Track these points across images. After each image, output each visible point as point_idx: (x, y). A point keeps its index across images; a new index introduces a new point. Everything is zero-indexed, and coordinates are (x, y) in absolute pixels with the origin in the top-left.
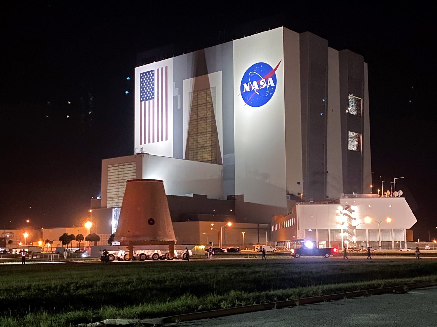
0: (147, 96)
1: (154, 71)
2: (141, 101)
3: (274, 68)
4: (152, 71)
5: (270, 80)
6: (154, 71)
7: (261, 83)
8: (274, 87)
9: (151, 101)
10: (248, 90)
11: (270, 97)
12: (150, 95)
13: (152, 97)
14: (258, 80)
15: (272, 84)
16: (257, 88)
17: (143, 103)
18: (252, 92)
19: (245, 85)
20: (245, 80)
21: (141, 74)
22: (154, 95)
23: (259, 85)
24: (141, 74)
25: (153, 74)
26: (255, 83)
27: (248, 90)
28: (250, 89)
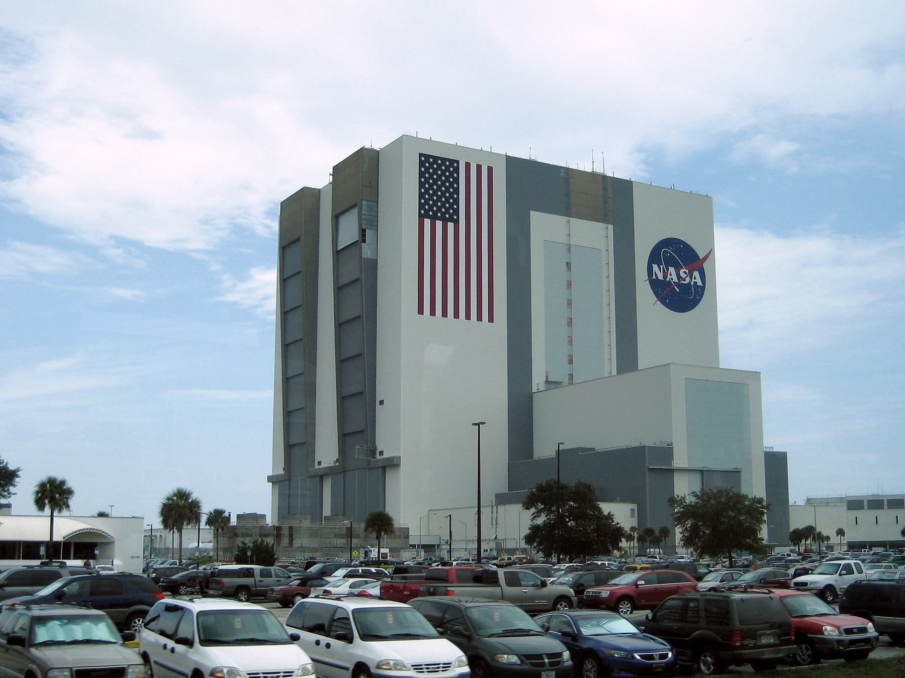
0: (439, 209)
1: (458, 162)
2: (421, 217)
4: (452, 162)
5: (696, 274)
6: (458, 162)
8: (703, 288)
10: (661, 277)
12: (447, 210)
13: (451, 216)
14: (678, 268)
15: (700, 283)
19: (655, 267)
21: (421, 155)
22: (457, 212)
24: (421, 155)
25: (457, 170)
26: (672, 270)
27: (661, 277)
28: (665, 277)
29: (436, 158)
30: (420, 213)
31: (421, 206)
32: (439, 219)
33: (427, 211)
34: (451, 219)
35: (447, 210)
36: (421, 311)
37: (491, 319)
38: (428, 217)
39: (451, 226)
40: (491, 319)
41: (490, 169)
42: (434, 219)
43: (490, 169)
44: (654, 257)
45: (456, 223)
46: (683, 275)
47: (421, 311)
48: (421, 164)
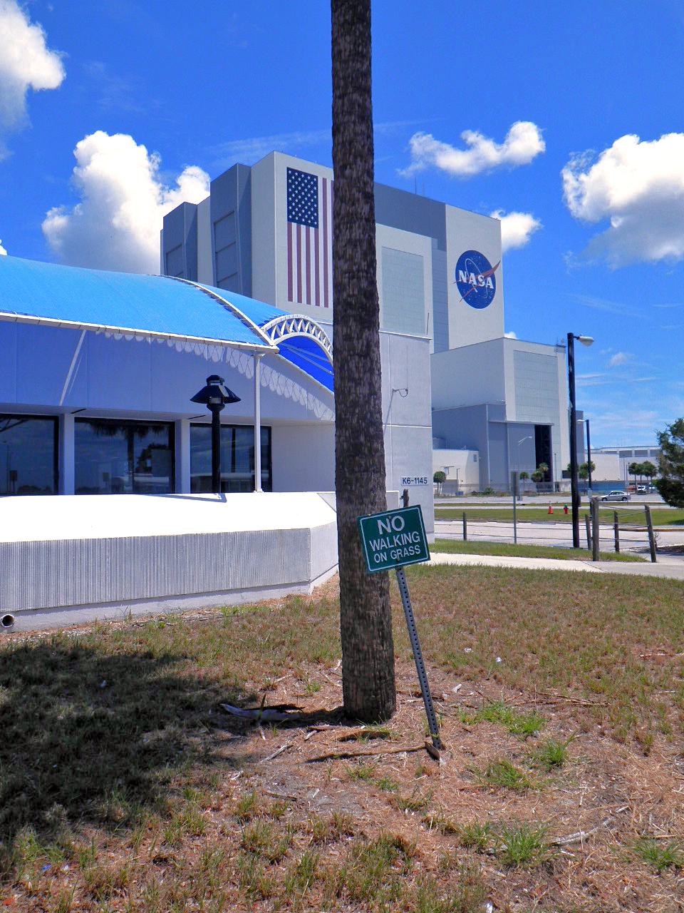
1: (317, 177)
2: (289, 220)
3: (493, 266)
4: (313, 177)
5: (489, 279)
6: (317, 177)
9: (312, 229)
10: (465, 281)
14: (476, 274)
15: (492, 287)
16: (475, 283)
17: (294, 225)
19: (461, 272)
21: (288, 169)
24: (288, 169)
25: (316, 184)
26: (472, 275)
27: (465, 281)
28: (468, 281)
29: (300, 173)
30: (288, 218)
31: (289, 212)
32: (304, 224)
33: (294, 217)
34: (312, 225)
35: (309, 218)
36: (290, 299)
38: (295, 221)
42: (299, 222)
44: (461, 265)
45: (316, 227)
46: (481, 280)
47: (290, 299)
48: (289, 177)
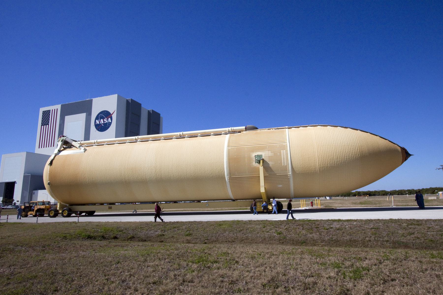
2: (42, 126)
5: (110, 119)
7: (105, 120)
8: (111, 123)
10: (98, 123)
11: (108, 127)
14: (103, 119)
15: (110, 121)
16: (103, 122)
18: (100, 125)
19: (97, 121)
20: (97, 118)
23: (104, 121)
26: (102, 120)
27: (98, 123)
31: (42, 123)
36: (39, 148)
37: (53, 146)
39: (47, 126)
40: (53, 146)
41: (57, 109)
43: (57, 109)
45: (48, 125)
47: (39, 148)
48: (43, 113)
